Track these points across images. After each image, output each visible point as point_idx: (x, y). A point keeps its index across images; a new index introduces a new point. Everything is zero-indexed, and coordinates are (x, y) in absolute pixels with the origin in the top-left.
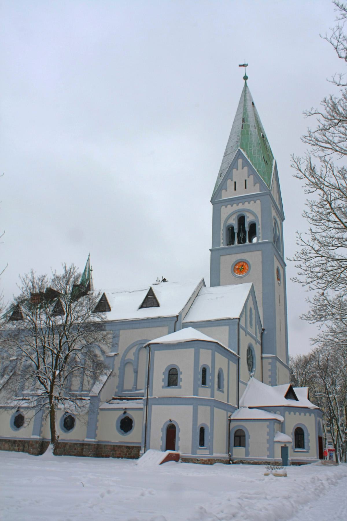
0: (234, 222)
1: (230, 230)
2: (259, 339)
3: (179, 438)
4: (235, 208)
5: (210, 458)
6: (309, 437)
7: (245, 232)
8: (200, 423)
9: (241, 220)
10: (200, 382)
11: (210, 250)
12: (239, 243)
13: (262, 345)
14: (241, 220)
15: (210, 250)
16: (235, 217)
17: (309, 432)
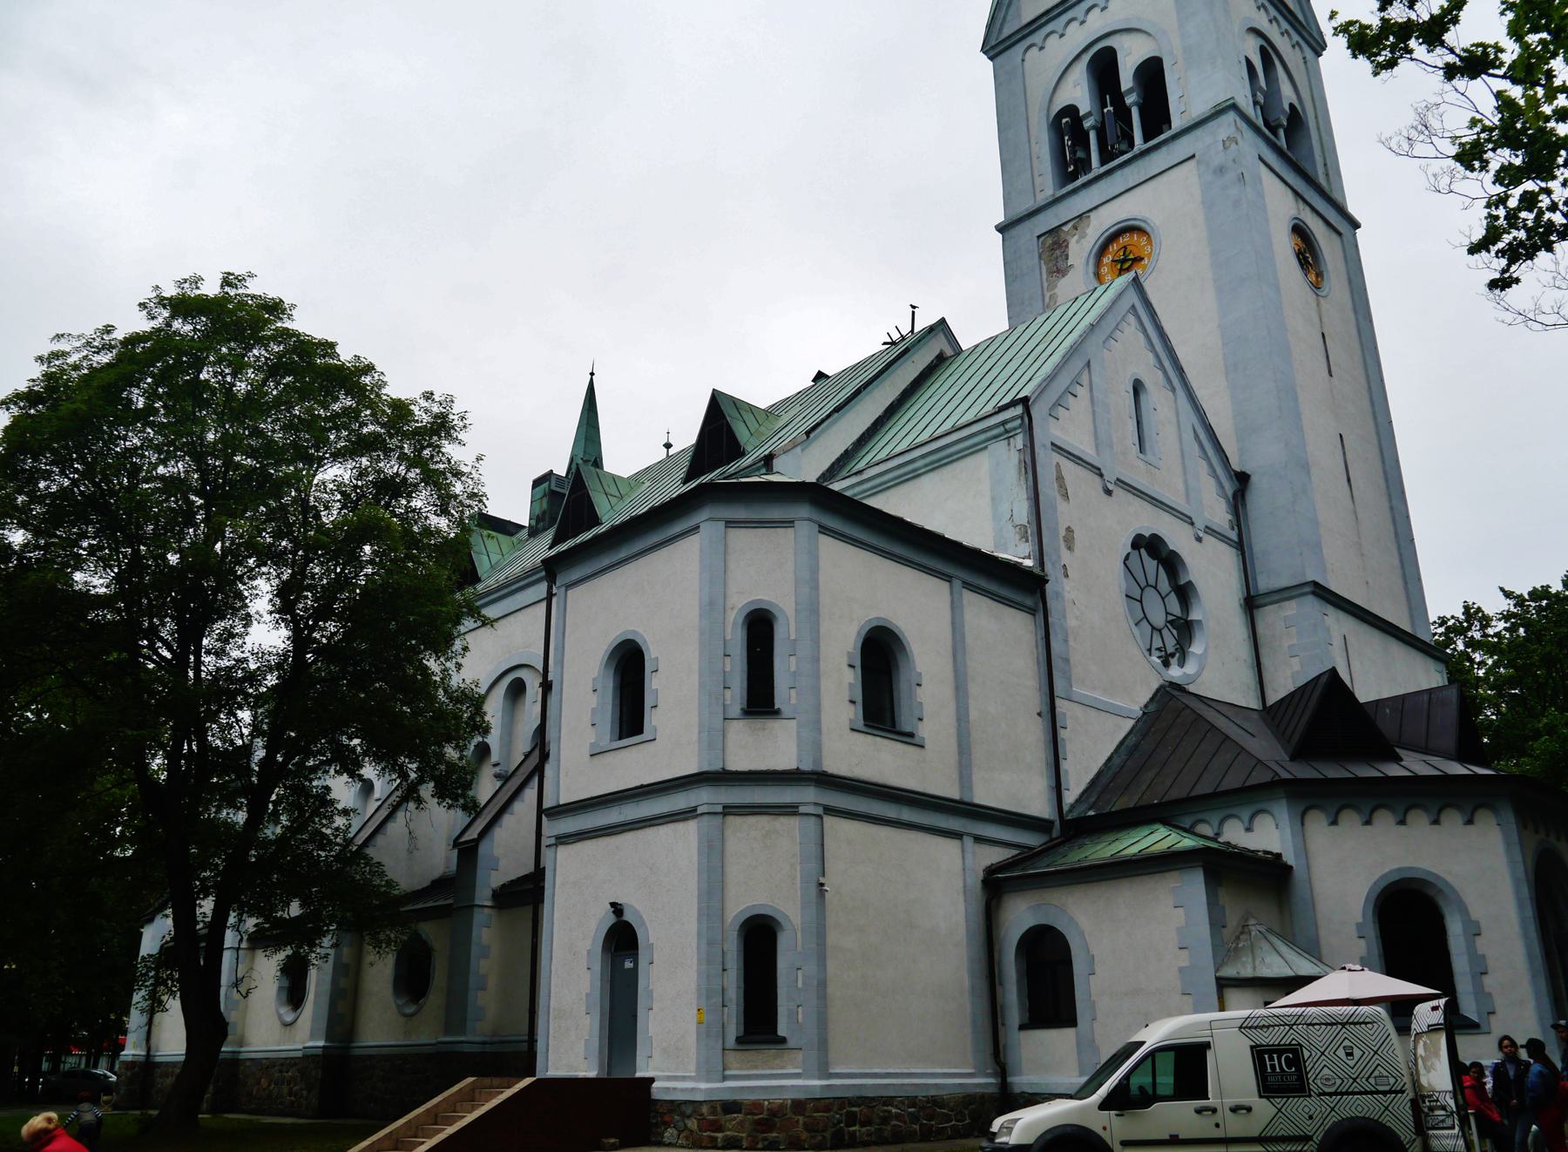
0: (1079, 92)
1: (1067, 124)
2: (1220, 515)
3: (650, 994)
4: (1076, 36)
5: (801, 1096)
6: (1482, 945)
7: (1123, 113)
8: (739, 905)
9: (1103, 66)
10: (736, 696)
11: (1001, 229)
12: (1106, 157)
13: (1241, 546)
14: (1103, 66)
15: (1001, 229)
16: (1080, 73)
17: (1477, 911)
